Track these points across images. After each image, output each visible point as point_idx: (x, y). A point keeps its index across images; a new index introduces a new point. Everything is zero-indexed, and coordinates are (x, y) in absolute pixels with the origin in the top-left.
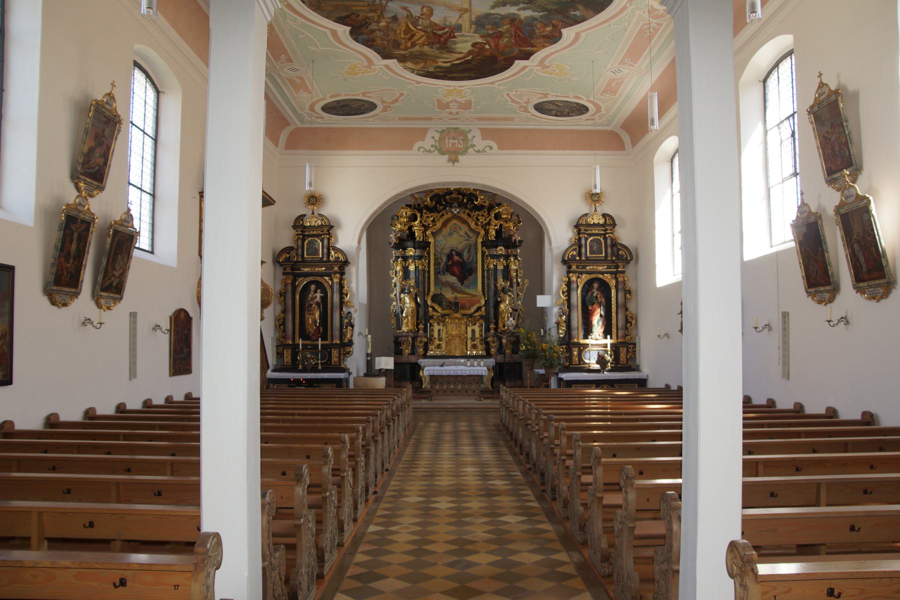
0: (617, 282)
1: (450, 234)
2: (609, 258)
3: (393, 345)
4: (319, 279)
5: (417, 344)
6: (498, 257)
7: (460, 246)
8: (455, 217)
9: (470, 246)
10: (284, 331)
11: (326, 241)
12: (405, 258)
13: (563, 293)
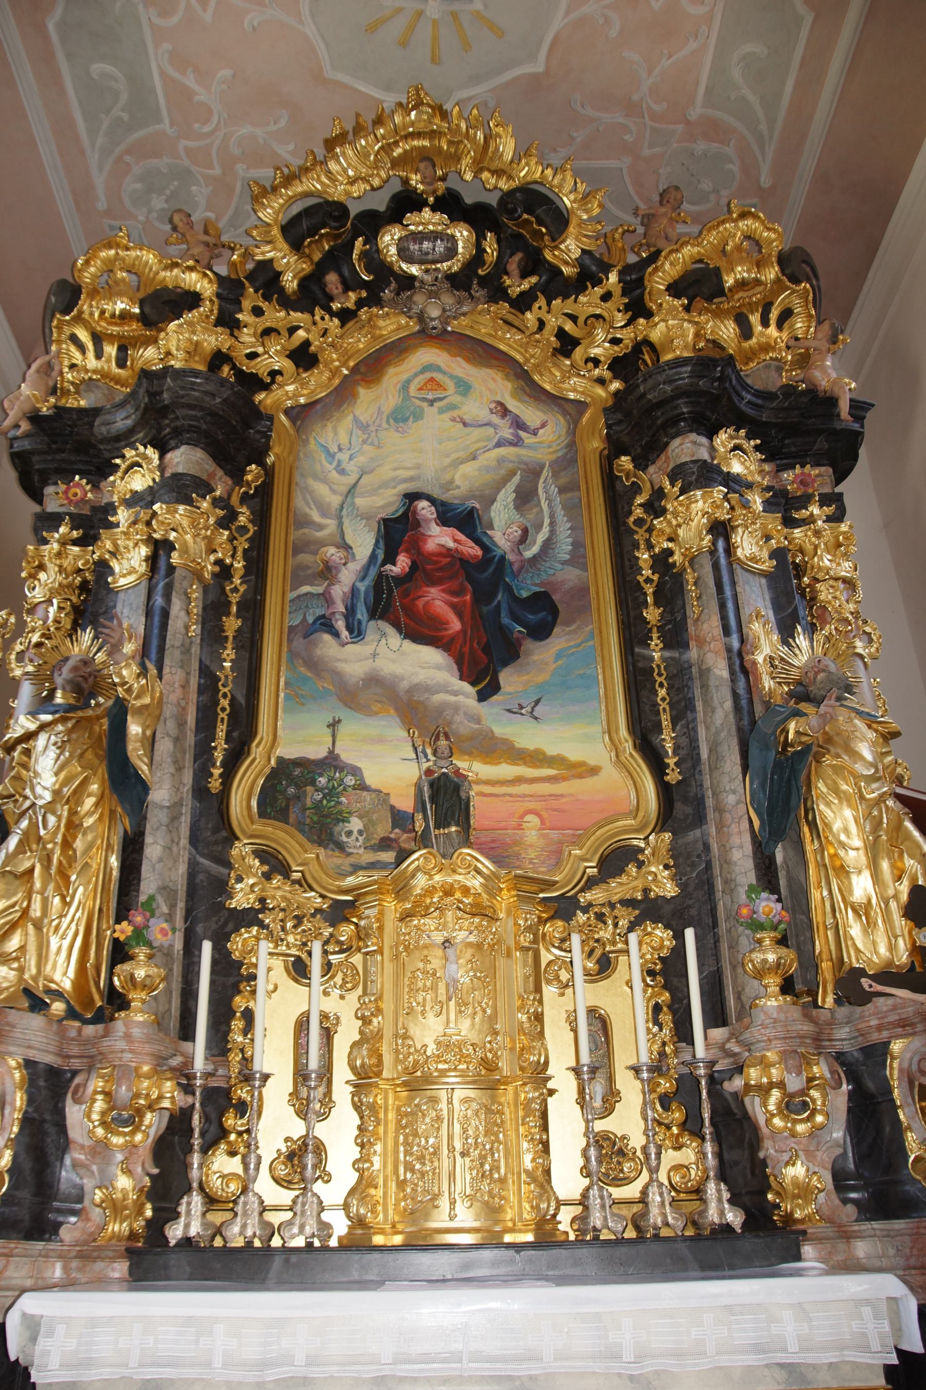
1: (401, 417)
5: (83, 1118)
9: (533, 472)
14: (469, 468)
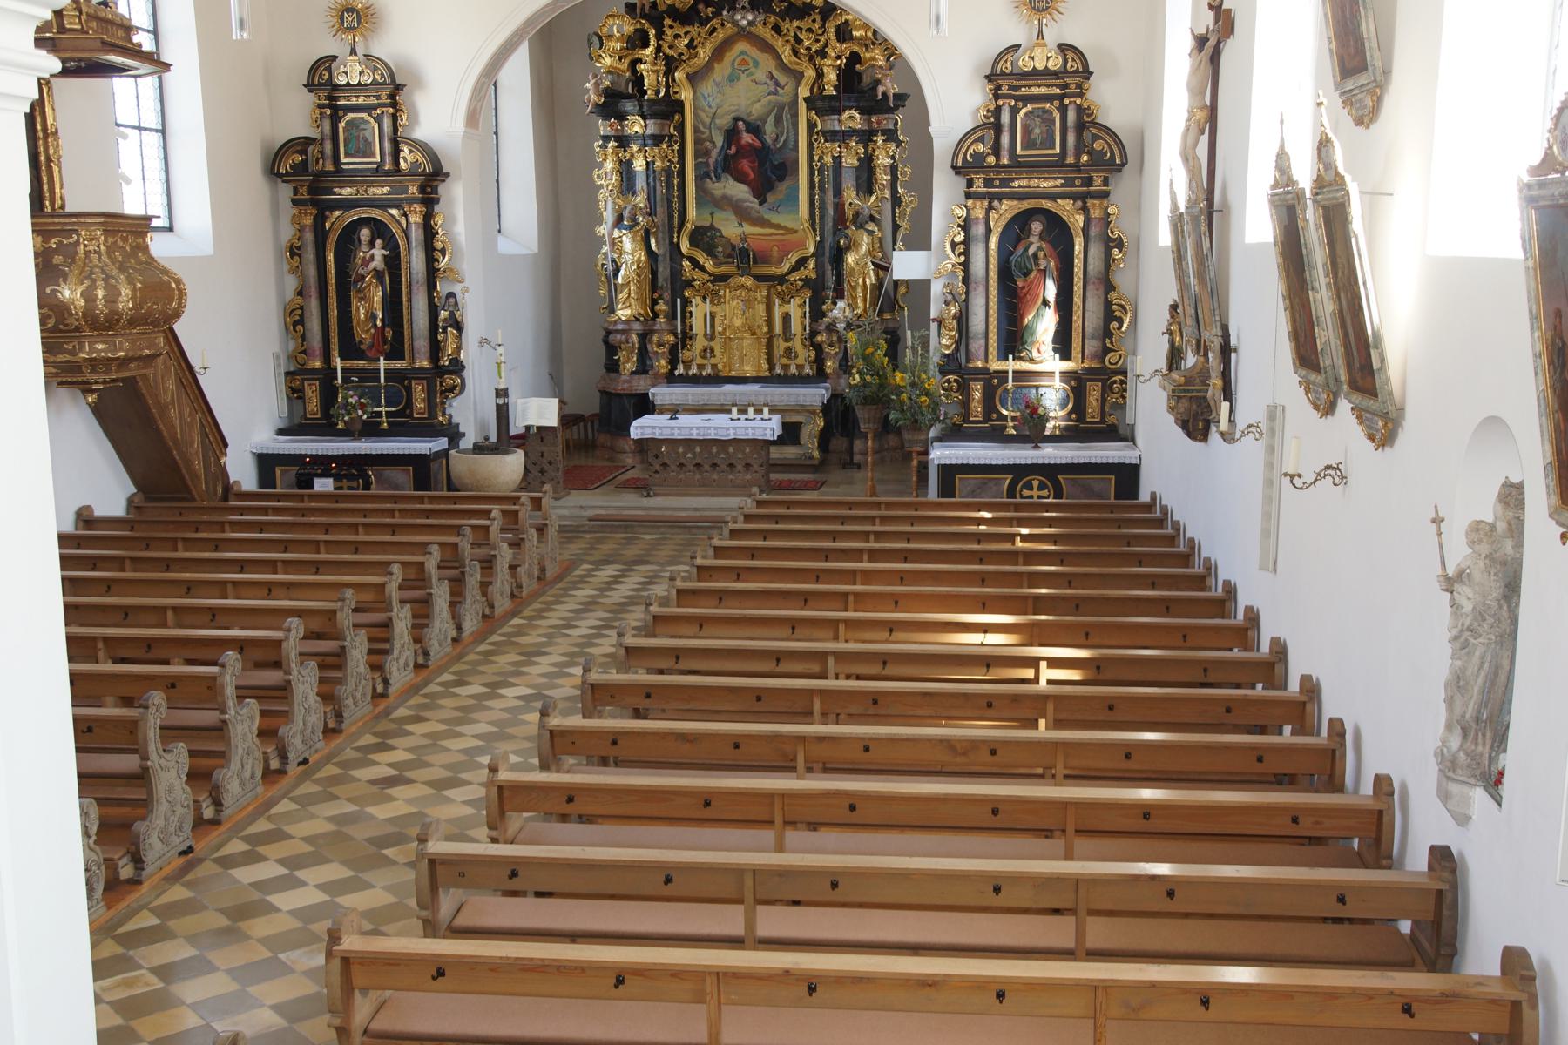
0: (1088, 221)
1: (732, 79)
2: (1070, 160)
3: (602, 350)
4: (376, 214)
5: (653, 348)
6: (841, 137)
7: (757, 110)
8: (744, 34)
9: (781, 108)
10: (303, 338)
11: (387, 123)
12: (623, 141)
13: (954, 245)
14: (758, 106)
